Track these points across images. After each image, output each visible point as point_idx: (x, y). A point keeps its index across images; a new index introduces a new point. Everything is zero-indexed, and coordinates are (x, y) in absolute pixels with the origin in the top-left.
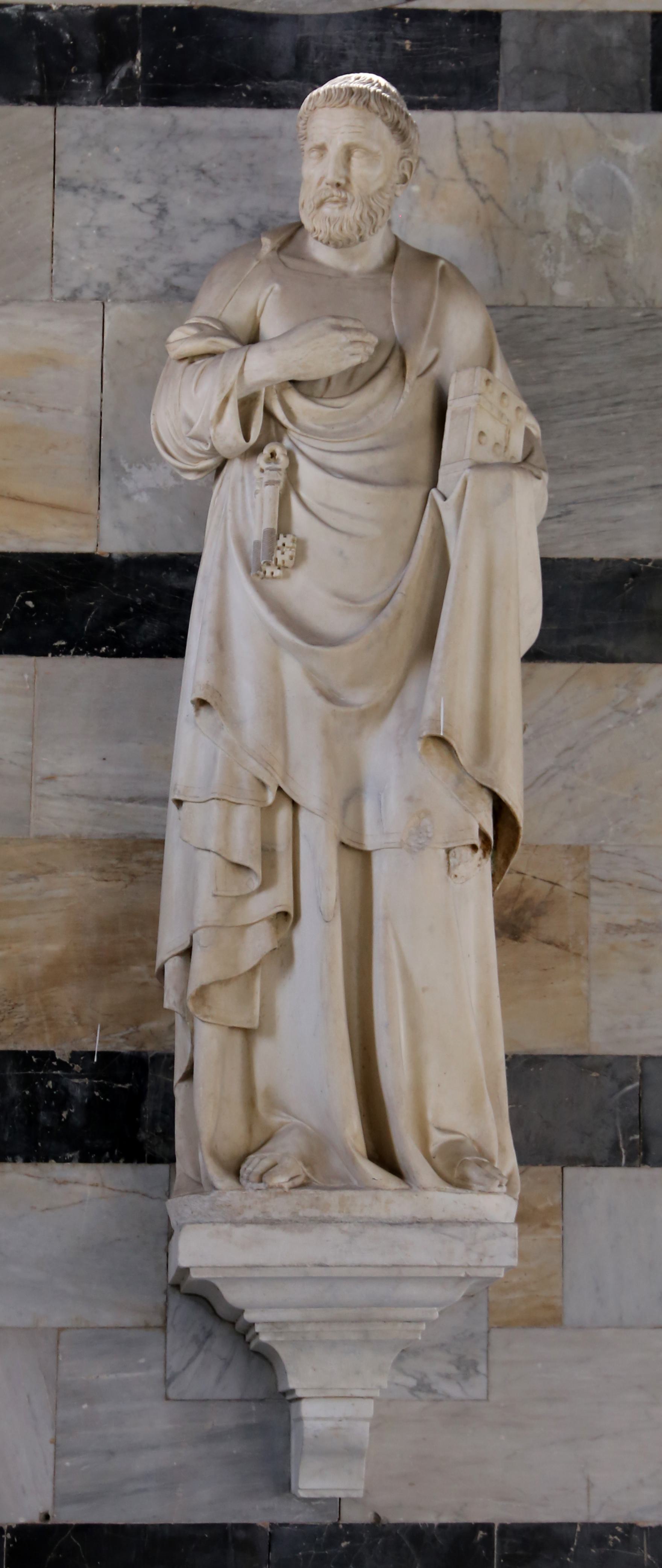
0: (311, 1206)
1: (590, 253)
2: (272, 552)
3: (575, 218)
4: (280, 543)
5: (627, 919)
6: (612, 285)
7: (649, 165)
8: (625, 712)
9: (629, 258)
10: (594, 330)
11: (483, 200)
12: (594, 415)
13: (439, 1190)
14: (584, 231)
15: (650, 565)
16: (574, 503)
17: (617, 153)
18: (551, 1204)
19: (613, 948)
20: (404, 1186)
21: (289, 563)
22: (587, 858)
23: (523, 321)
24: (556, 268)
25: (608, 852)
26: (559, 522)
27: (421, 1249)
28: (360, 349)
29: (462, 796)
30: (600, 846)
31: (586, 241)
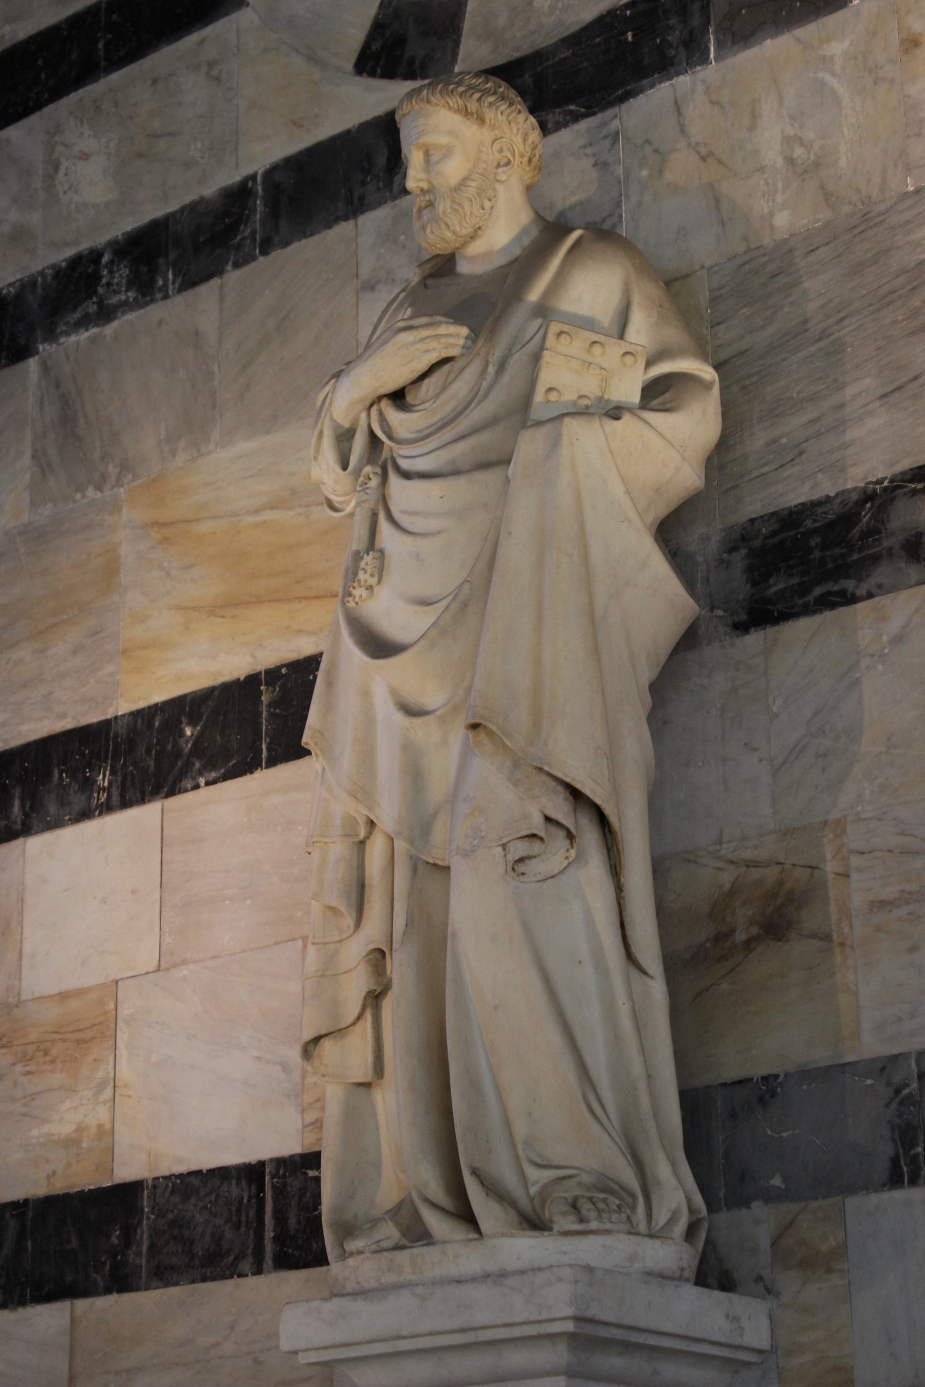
0: (389, 1270)
1: (805, 171)
2: (355, 574)
3: (788, 141)
4: (363, 564)
5: (889, 892)
6: (827, 196)
7: (855, 58)
8: (872, 656)
9: (843, 163)
10: (813, 250)
11: (704, 159)
12: (820, 339)
13: (503, 1235)
14: (799, 152)
15: (886, 483)
16: (806, 441)
17: (824, 59)
18: (834, 1244)
19: (878, 929)
20: (476, 1236)
21: (373, 581)
22: (844, 831)
23: (747, 267)
24: (774, 201)
25: (865, 819)
26: (793, 466)
27: (487, 1308)
28: (434, 344)
29: (516, 784)
30: (857, 814)
31: (800, 162)
